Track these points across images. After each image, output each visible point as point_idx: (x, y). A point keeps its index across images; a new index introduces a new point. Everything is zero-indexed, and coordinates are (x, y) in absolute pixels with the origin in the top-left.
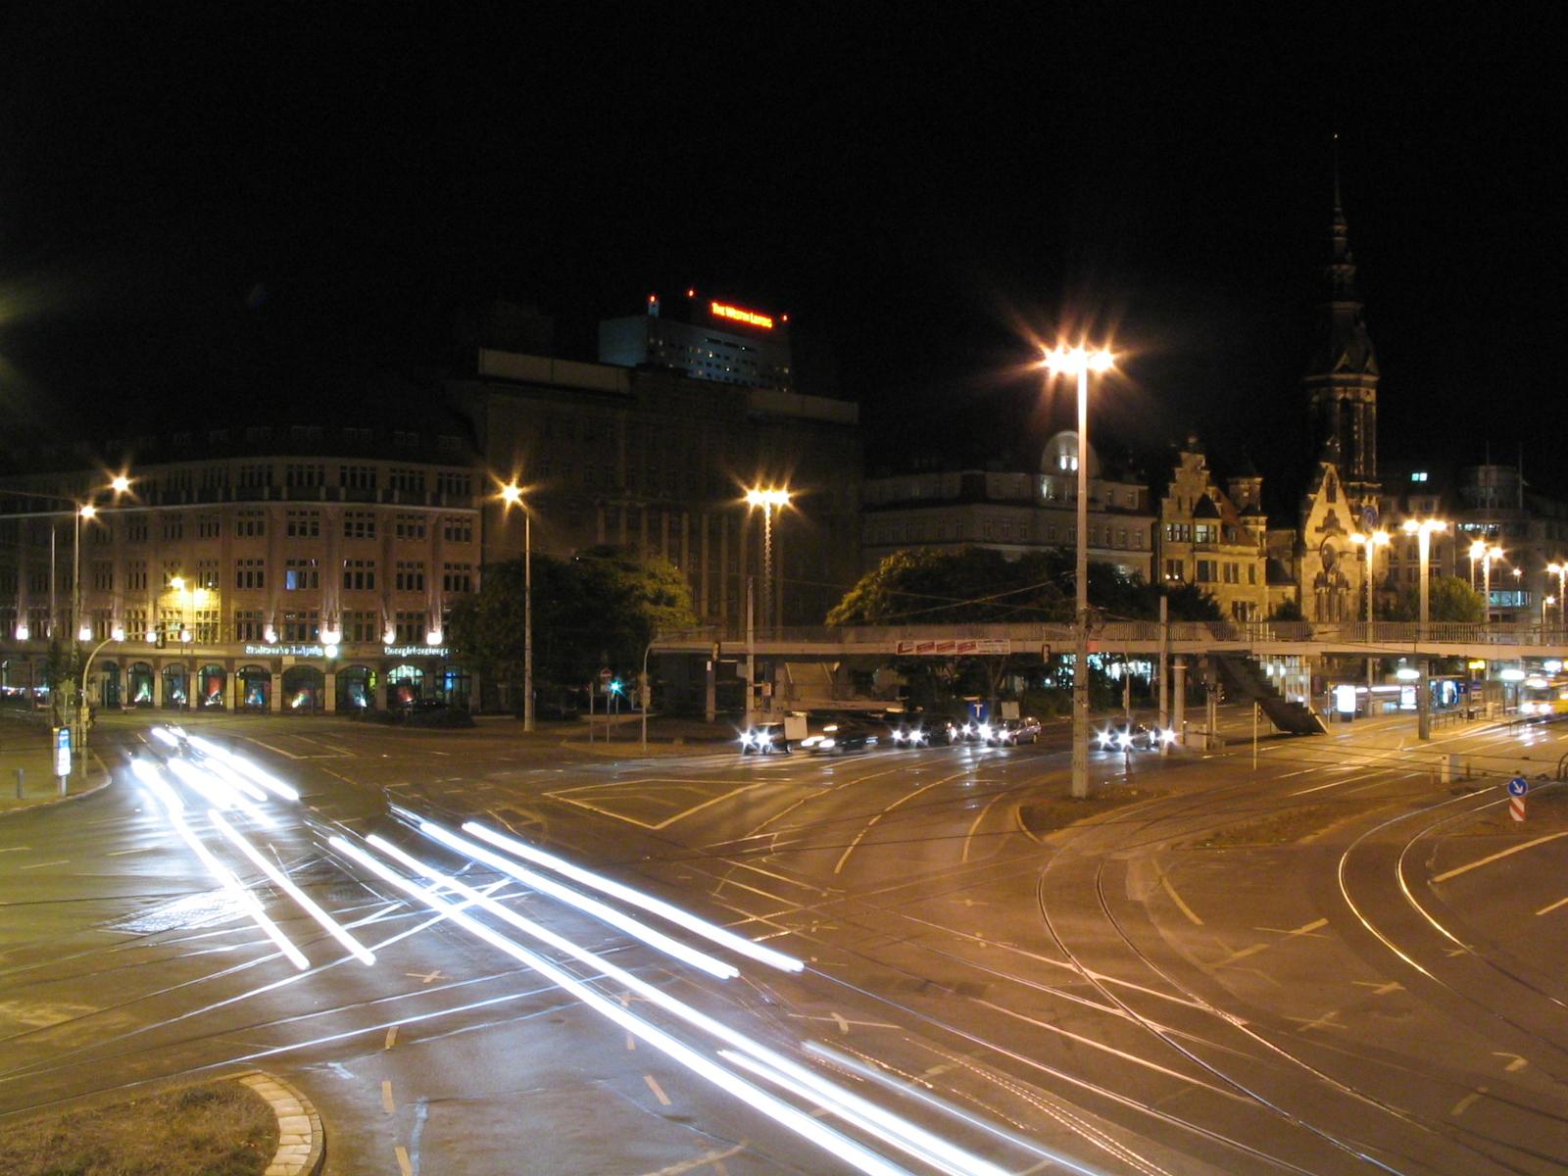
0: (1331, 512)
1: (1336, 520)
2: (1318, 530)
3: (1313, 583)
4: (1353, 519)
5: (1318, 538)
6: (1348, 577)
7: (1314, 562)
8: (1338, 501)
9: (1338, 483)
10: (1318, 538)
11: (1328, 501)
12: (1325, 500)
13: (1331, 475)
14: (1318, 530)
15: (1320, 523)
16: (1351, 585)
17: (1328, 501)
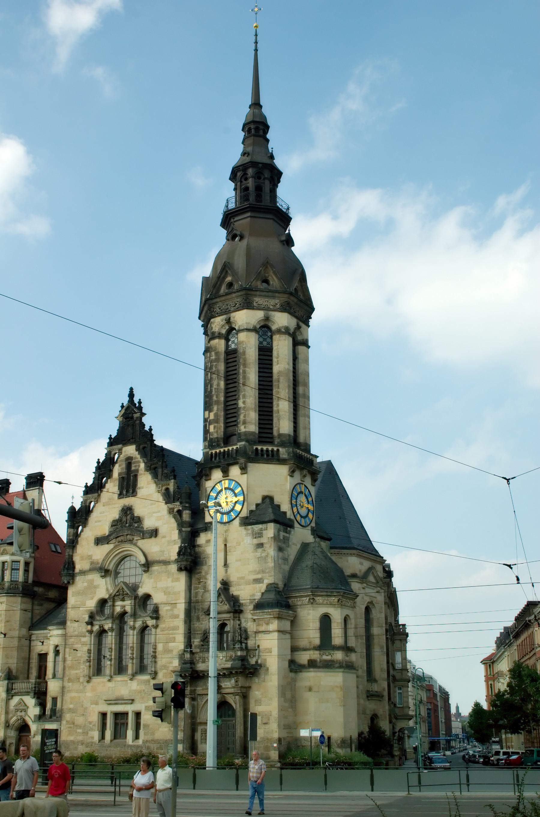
0: (127, 511)
1: (139, 520)
2: (99, 541)
3: (86, 618)
4: (171, 511)
5: (100, 553)
6: (157, 598)
7: (92, 587)
8: (141, 492)
9: (142, 465)
10: (100, 553)
11: (121, 495)
12: (116, 496)
13: (129, 461)
14: (99, 541)
15: (105, 529)
16: (163, 610)
17: (121, 495)
